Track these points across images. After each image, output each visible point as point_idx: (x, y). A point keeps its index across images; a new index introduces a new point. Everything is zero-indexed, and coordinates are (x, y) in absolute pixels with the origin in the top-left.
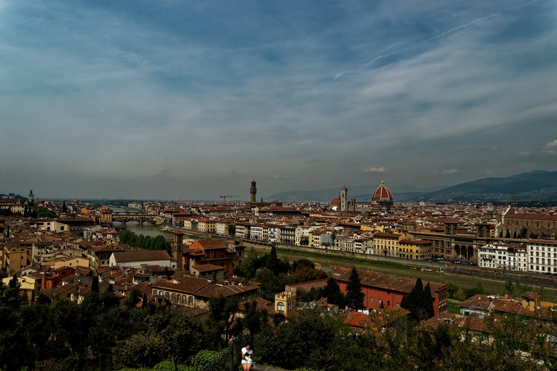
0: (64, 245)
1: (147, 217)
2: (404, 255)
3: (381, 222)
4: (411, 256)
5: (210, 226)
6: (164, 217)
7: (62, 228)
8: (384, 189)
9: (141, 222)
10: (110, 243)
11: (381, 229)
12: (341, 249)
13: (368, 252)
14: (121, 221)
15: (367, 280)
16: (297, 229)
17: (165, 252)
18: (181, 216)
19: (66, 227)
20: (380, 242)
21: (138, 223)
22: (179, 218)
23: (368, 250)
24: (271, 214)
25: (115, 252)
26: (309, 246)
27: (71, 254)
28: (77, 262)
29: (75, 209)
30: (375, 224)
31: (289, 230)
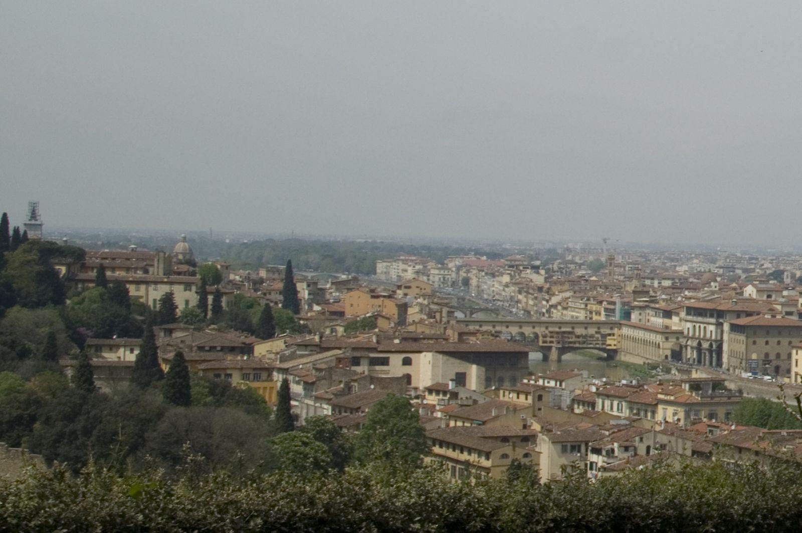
1: (579, 331)
6: (667, 333)
7: (461, 379)
18: (768, 330)
19: (474, 372)
22: (761, 341)
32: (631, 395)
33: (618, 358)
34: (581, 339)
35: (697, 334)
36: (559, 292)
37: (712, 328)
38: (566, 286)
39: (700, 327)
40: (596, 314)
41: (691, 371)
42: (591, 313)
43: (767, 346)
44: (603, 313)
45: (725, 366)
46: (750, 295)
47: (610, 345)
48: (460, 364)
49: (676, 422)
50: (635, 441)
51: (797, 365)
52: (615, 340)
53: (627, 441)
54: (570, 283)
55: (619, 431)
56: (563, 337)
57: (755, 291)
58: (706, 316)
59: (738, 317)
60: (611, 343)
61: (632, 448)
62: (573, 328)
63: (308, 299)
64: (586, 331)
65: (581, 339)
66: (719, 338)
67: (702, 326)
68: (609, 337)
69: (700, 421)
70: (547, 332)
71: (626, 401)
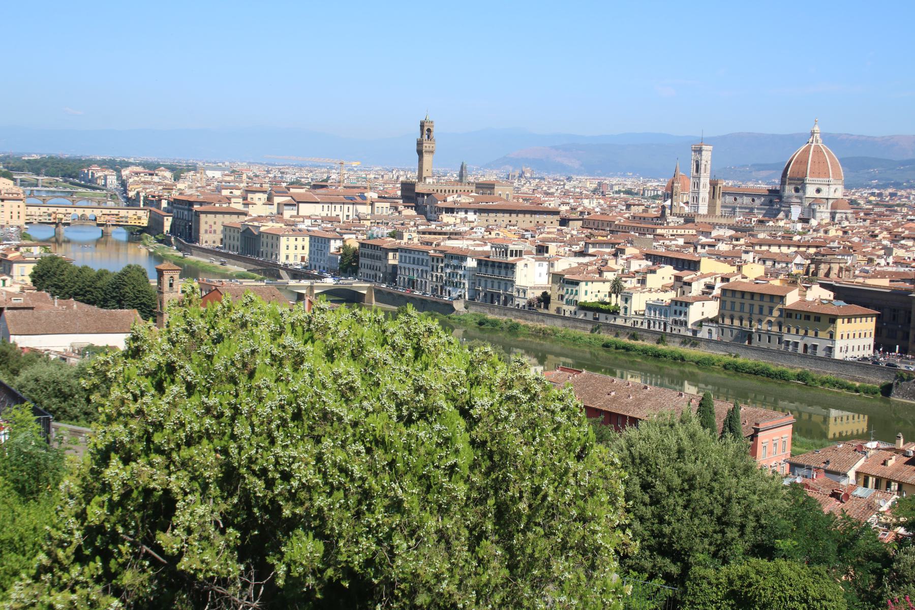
2: (796, 344)
3: (775, 249)
4: (815, 347)
5: (292, 247)
8: (818, 151)
11: (754, 271)
12: (635, 323)
13: (703, 334)
15: (614, 399)
16: (520, 265)
20: (737, 307)
23: (705, 329)
24: (471, 216)
26: (552, 310)
30: (744, 256)
31: (500, 265)
34: (124, 219)
37: (186, 213)
65: (124, 219)
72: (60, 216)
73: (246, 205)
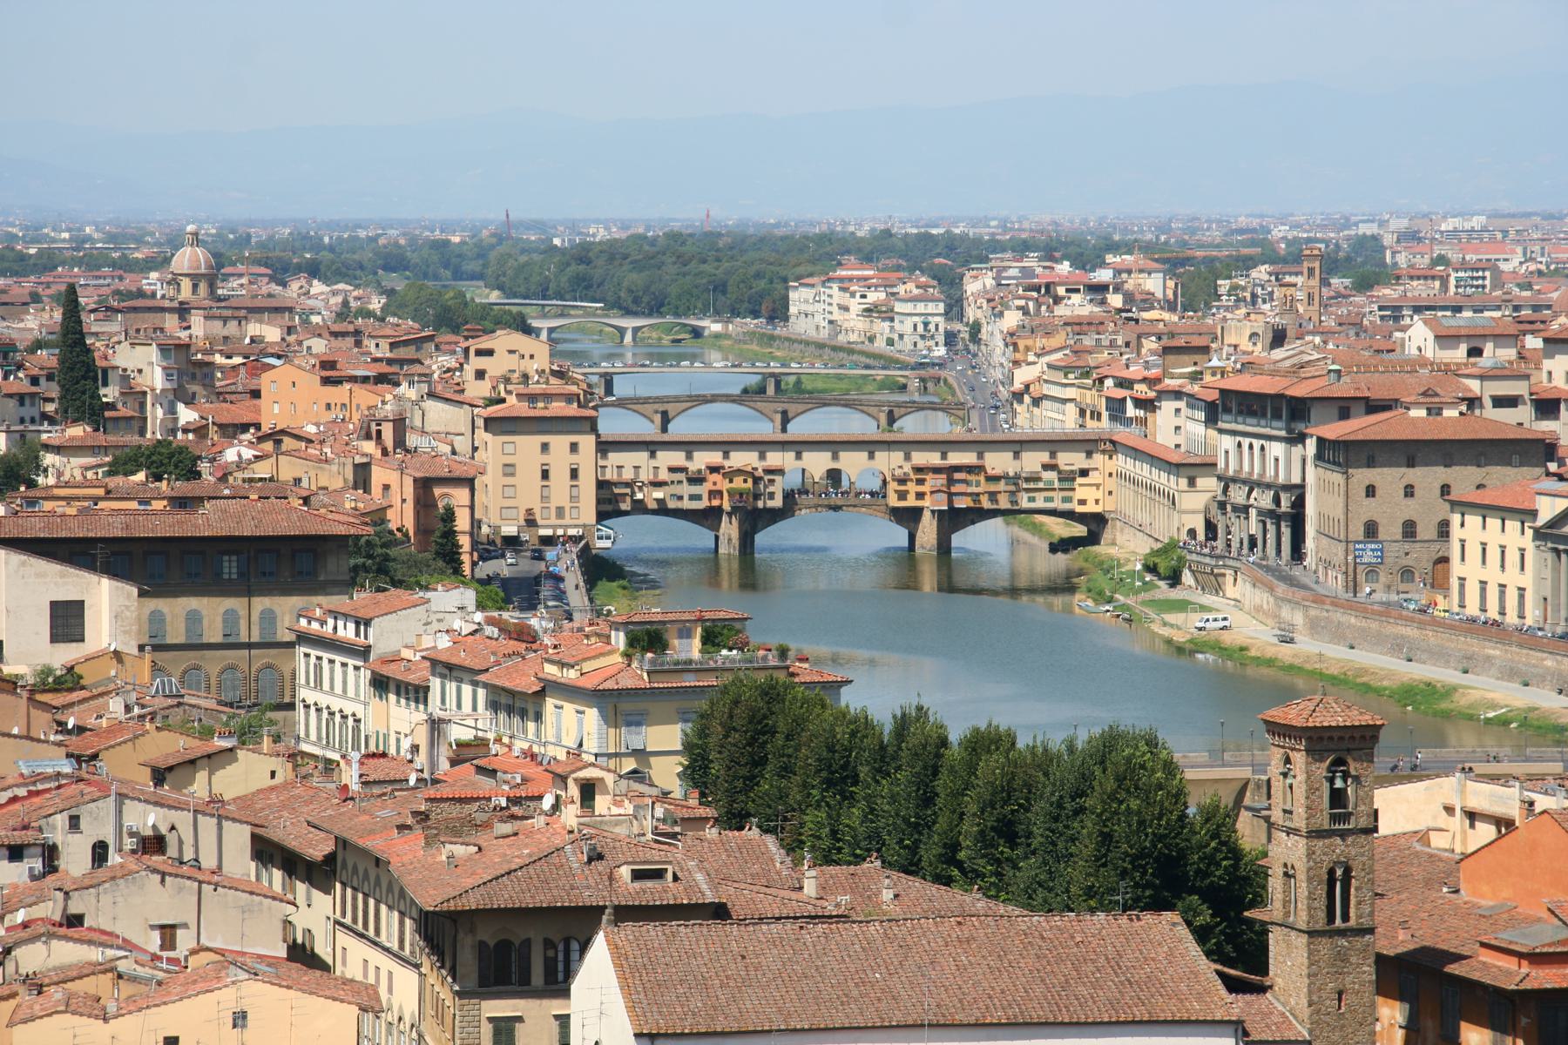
0: (99, 823)
1: (998, 462)
7: (67, 620)
9: (928, 531)
10: (571, 815)
14: (709, 518)
17: (1168, 941)
18: (1411, 452)
19: (108, 603)
21: (899, 536)
25: (625, 913)
27: (168, 932)
28: (240, 1019)
29: (190, 372)
32: (498, 663)
33: (1107, 536)
35: (1246, 468)
36: (1038, 355)
38: (1058, 340)
39: (1251, 447)
40: (1092, 418)
41: (1224, 575)
42: (1082, 413)
43: (1410, 501)
44: (1105, 415)
45: (1310, 561)
46: (1420, 349)
47: (1082, 502)
48: (62, 576)
49: (409, 757)
50: (54, 827)
51: (1463, 559)
52: (1098, 486)
53: (25, 827)
54: (1069, 329)
55: (31, 794)
56: (951, 482)
57: (1431, 337)
58: (1264, 415)
59: (1344, 414)
60: (1088, 497)
61: (39, 850)
62: (980, 456)
63: (163, 390)
64: (1017, 463)
65: (1001, 486)
66: (1296, 480)
67: (1257, 443)
68: (1080, 480)
69: (482, 751)
70: (907, 468)
71: (485, 685)
72: (738, 483)
73: (1547, 407)
